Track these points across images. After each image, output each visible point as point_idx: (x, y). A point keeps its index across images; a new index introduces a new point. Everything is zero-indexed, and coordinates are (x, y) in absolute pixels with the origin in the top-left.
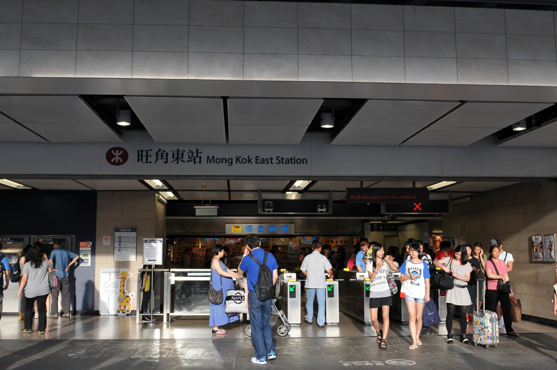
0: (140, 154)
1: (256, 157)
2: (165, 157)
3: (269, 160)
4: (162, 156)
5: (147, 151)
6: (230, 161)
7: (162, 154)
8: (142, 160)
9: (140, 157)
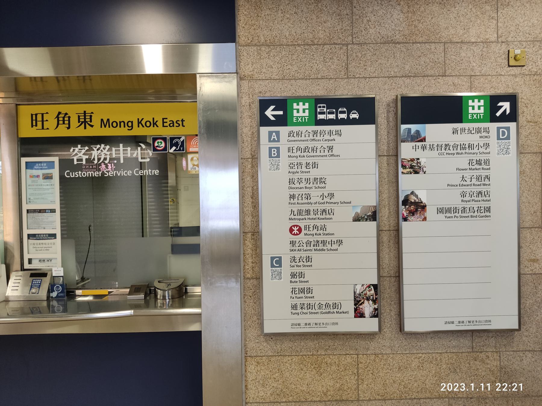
0: (34, 118)
1: (163, 119)
2: (66, 122)
3: (180, 123)
4: (64, 121)
5: (43, 114)
6: (130, 124)
7: (64, 118)
8: (36, 125)
9: (34, 122)
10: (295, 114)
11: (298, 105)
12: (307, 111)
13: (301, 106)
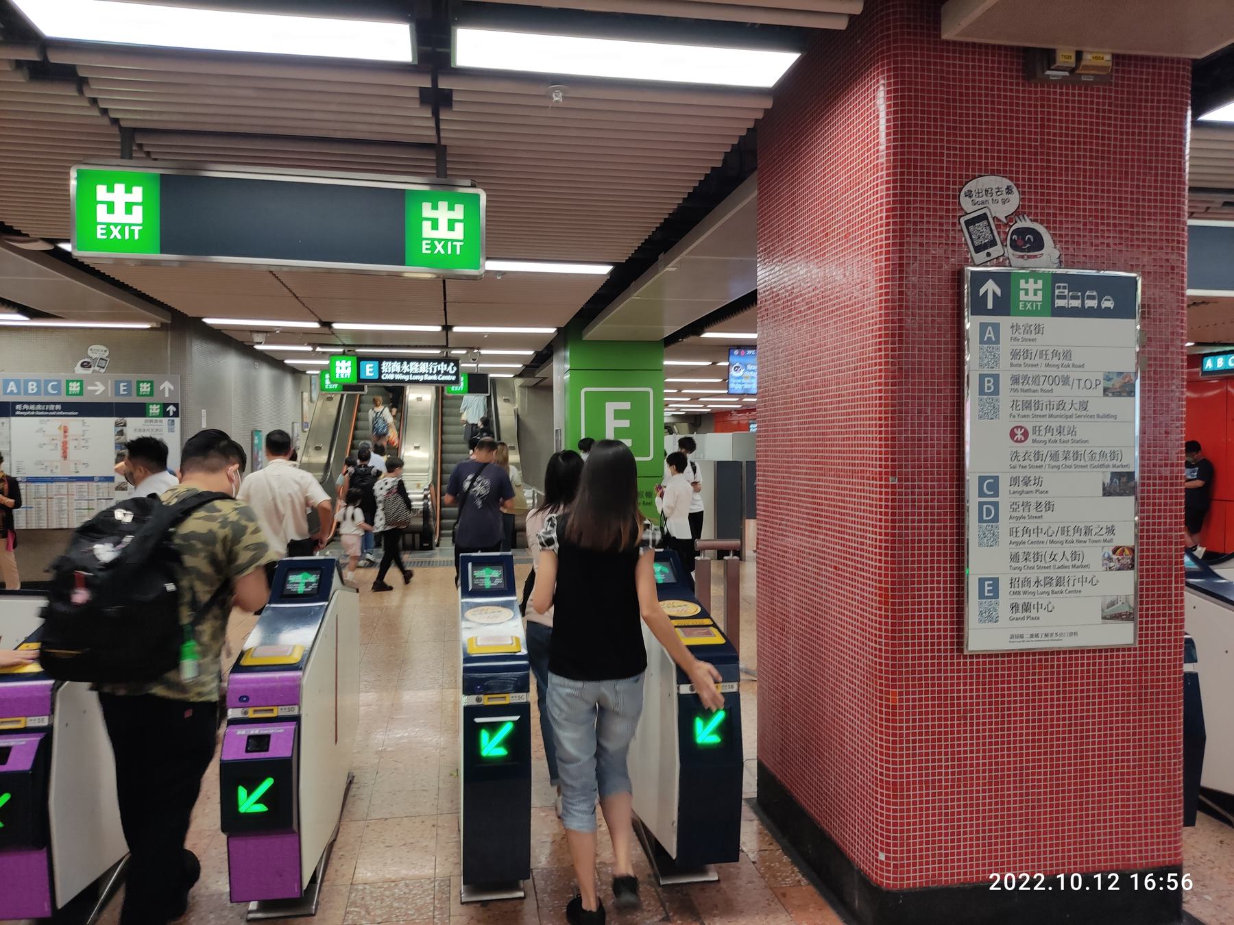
10: (1022, 297)
11: (1027, 282)
12: (1040, 293)
13: (1031, 285)
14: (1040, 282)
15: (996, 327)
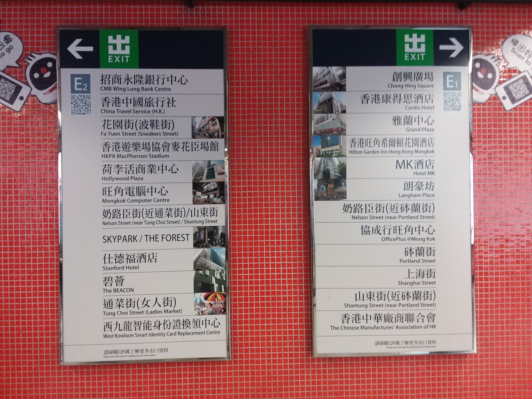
11: (115, 38)
13: (119, 41)
14: (127, 38)
15: (86, 79)
